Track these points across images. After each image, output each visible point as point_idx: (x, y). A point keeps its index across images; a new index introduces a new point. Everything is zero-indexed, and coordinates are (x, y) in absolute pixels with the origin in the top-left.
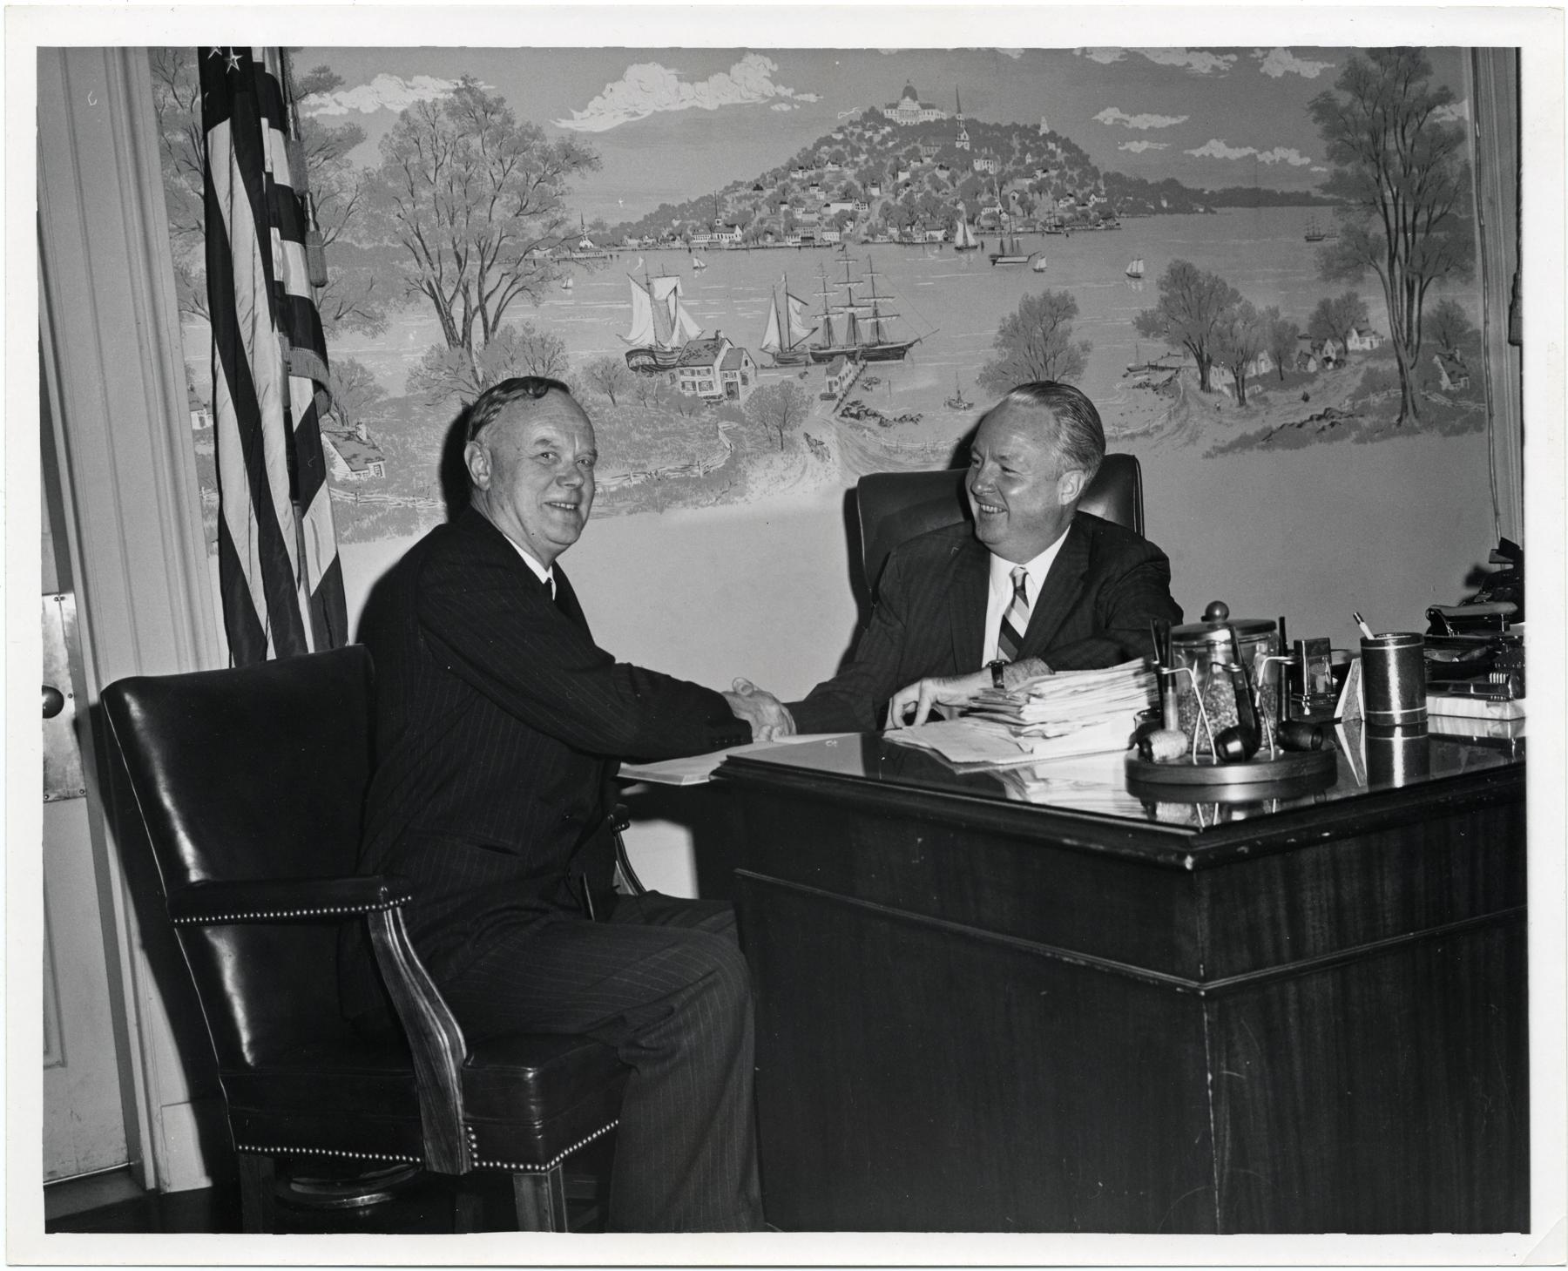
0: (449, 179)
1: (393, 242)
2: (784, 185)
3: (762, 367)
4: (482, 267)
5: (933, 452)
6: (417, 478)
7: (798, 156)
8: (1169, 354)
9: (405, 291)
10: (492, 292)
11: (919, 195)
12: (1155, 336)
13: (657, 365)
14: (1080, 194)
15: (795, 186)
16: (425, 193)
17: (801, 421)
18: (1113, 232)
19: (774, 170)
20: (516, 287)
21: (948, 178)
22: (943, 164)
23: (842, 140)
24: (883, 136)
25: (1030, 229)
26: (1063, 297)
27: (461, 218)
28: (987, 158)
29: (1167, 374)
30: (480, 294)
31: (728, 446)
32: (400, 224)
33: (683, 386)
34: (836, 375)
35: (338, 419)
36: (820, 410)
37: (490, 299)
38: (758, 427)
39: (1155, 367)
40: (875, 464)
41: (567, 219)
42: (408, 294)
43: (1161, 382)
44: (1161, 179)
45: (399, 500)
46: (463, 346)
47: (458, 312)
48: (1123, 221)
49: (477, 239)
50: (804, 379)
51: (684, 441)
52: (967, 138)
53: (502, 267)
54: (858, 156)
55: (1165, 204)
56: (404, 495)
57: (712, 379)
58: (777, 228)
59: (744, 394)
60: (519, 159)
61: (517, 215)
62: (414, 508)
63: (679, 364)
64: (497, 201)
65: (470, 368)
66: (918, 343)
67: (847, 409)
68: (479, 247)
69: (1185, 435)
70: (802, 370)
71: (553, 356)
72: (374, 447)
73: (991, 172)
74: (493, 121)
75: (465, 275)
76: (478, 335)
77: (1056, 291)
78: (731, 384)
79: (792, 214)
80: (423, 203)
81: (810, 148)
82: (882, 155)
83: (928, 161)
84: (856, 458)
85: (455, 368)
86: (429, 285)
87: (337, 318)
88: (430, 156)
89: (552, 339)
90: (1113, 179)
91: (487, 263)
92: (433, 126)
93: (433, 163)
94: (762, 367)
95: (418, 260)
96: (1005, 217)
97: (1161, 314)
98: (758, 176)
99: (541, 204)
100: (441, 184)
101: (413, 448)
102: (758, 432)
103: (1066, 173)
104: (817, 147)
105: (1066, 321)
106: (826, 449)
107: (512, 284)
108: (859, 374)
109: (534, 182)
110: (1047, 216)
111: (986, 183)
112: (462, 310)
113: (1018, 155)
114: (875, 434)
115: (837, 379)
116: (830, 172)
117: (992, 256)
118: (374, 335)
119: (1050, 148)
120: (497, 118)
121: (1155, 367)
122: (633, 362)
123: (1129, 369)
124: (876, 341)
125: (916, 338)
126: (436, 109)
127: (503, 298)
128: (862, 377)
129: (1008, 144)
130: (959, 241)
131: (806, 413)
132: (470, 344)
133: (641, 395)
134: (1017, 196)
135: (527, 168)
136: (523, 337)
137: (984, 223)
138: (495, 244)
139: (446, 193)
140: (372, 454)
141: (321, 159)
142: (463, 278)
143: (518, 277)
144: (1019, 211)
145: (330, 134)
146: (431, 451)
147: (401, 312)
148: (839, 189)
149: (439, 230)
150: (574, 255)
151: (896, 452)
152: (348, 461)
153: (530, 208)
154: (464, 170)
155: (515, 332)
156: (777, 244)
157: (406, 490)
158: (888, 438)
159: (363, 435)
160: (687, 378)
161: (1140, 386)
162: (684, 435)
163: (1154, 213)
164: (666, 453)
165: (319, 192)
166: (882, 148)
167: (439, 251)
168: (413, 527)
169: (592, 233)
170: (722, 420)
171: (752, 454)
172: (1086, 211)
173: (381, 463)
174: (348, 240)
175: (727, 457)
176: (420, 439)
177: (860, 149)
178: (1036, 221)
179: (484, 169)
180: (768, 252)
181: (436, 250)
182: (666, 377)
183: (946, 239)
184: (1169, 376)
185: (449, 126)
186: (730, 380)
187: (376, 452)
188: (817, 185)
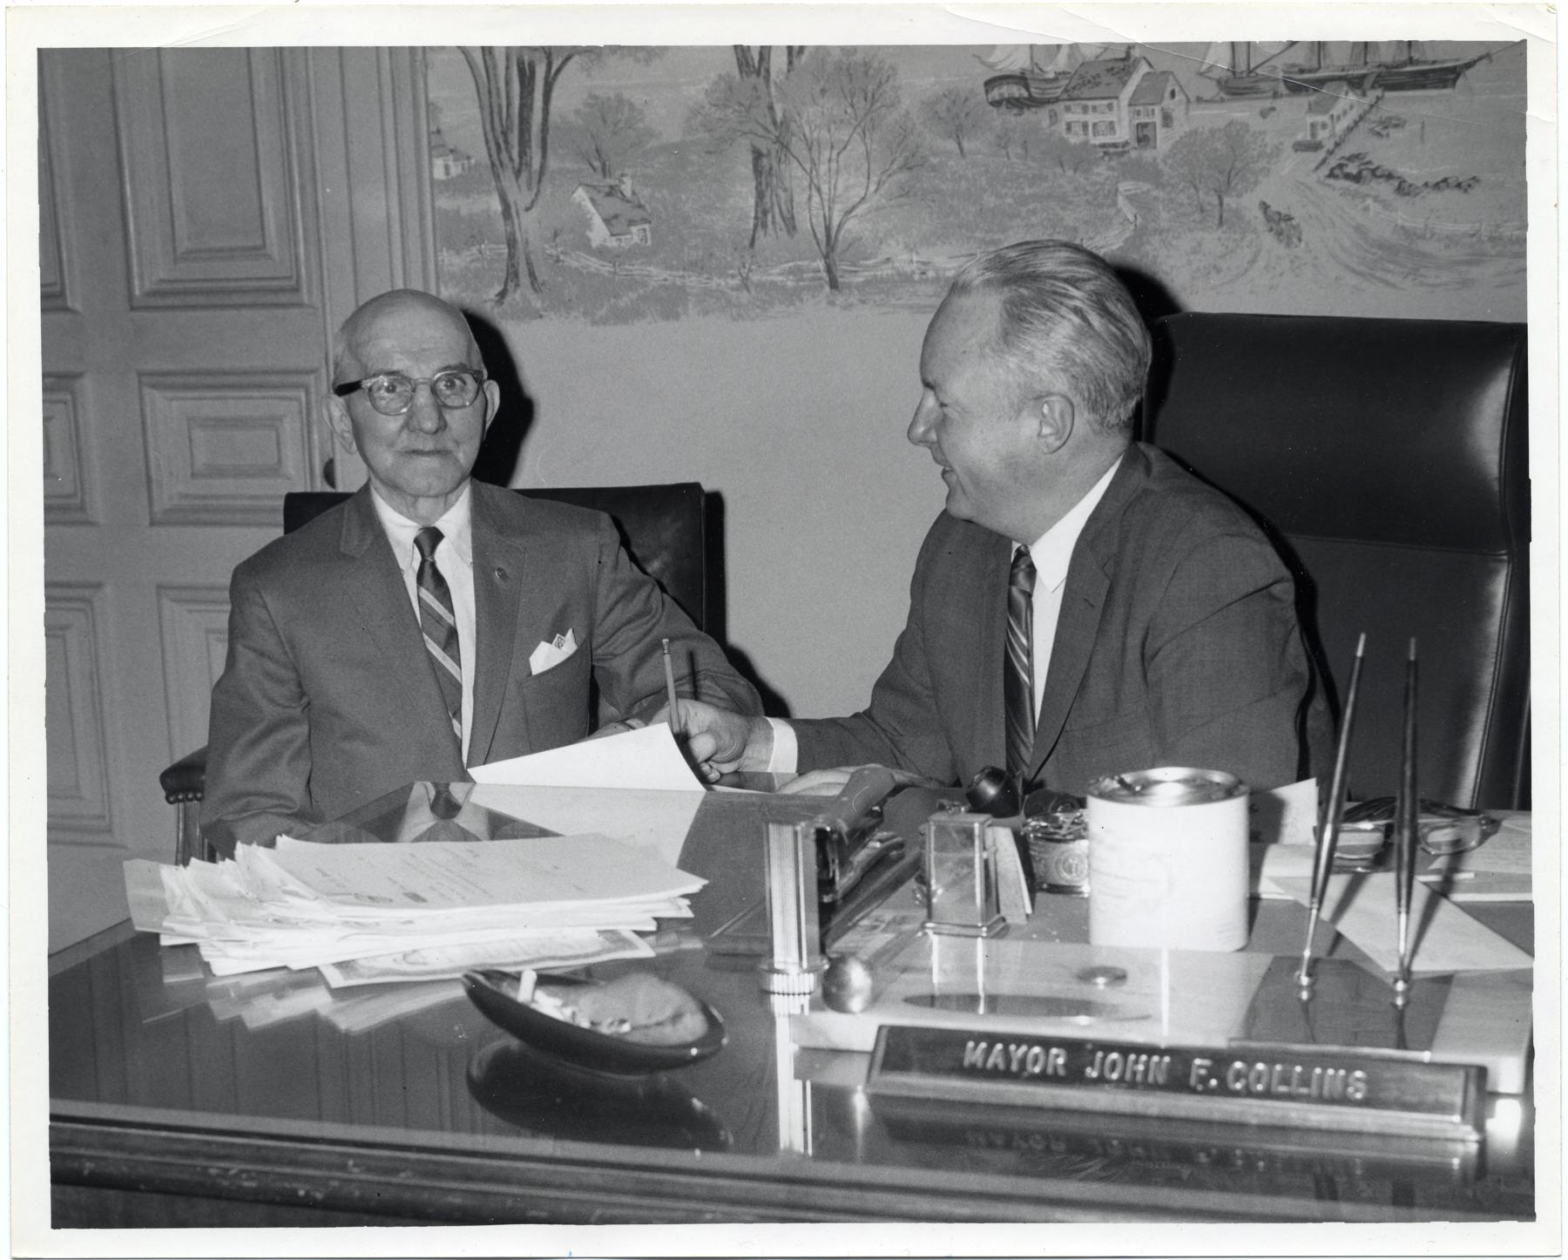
3: (1199, 100)
5: (1491, 239)
13: (1031, 98)
17: (1256, 183)
31: (1131, 218)
33: (1069, 128)
34: (1326, 112)
35: (599, 170)
36: (1291, 165)
38: (1182, 190)
40: (1380, 252)
45: (666, 274)
46: (758, 74)
50: (1268, 120)
51: (1063, 209)
56: (670, 268)
57: (1115, 119)
59: (1164, 140)
62: (682, 288)
63: (1065, 96)
66: (1485, 61)
67: (1340, 166)
70: (1268, 104)
72: (640, 206)
78: (1144, 126)
84: (1347, 244)
85: (747, 103)
89: (880, 63)
94: (1199, 100)
102: (1182, 198)
106: (1295, 228)
108: (1366, 113)
114: (1386, 205)
115: (1325, 118)
122: (995, 94)
124: (1404, 57)
125: (1484, 53)
128: (1373, 116)
131: (1266, 171)
132: (768, 71)
133: (1003, 141)
140: (637, 214)
146: (708, 213)
151: (1423, 237)
152: (607, 221)
158: (1405, 214)
159: (627, 188)
160: (1075, 116)
162: (1064, 201)
164: (1033, 226)
168: (680, 310)
170: (1125, 178)
171: (1168, 230)
173: (646, 226)
175: (1128, 234)
182: (1041, 116)
186: (1143, 120)
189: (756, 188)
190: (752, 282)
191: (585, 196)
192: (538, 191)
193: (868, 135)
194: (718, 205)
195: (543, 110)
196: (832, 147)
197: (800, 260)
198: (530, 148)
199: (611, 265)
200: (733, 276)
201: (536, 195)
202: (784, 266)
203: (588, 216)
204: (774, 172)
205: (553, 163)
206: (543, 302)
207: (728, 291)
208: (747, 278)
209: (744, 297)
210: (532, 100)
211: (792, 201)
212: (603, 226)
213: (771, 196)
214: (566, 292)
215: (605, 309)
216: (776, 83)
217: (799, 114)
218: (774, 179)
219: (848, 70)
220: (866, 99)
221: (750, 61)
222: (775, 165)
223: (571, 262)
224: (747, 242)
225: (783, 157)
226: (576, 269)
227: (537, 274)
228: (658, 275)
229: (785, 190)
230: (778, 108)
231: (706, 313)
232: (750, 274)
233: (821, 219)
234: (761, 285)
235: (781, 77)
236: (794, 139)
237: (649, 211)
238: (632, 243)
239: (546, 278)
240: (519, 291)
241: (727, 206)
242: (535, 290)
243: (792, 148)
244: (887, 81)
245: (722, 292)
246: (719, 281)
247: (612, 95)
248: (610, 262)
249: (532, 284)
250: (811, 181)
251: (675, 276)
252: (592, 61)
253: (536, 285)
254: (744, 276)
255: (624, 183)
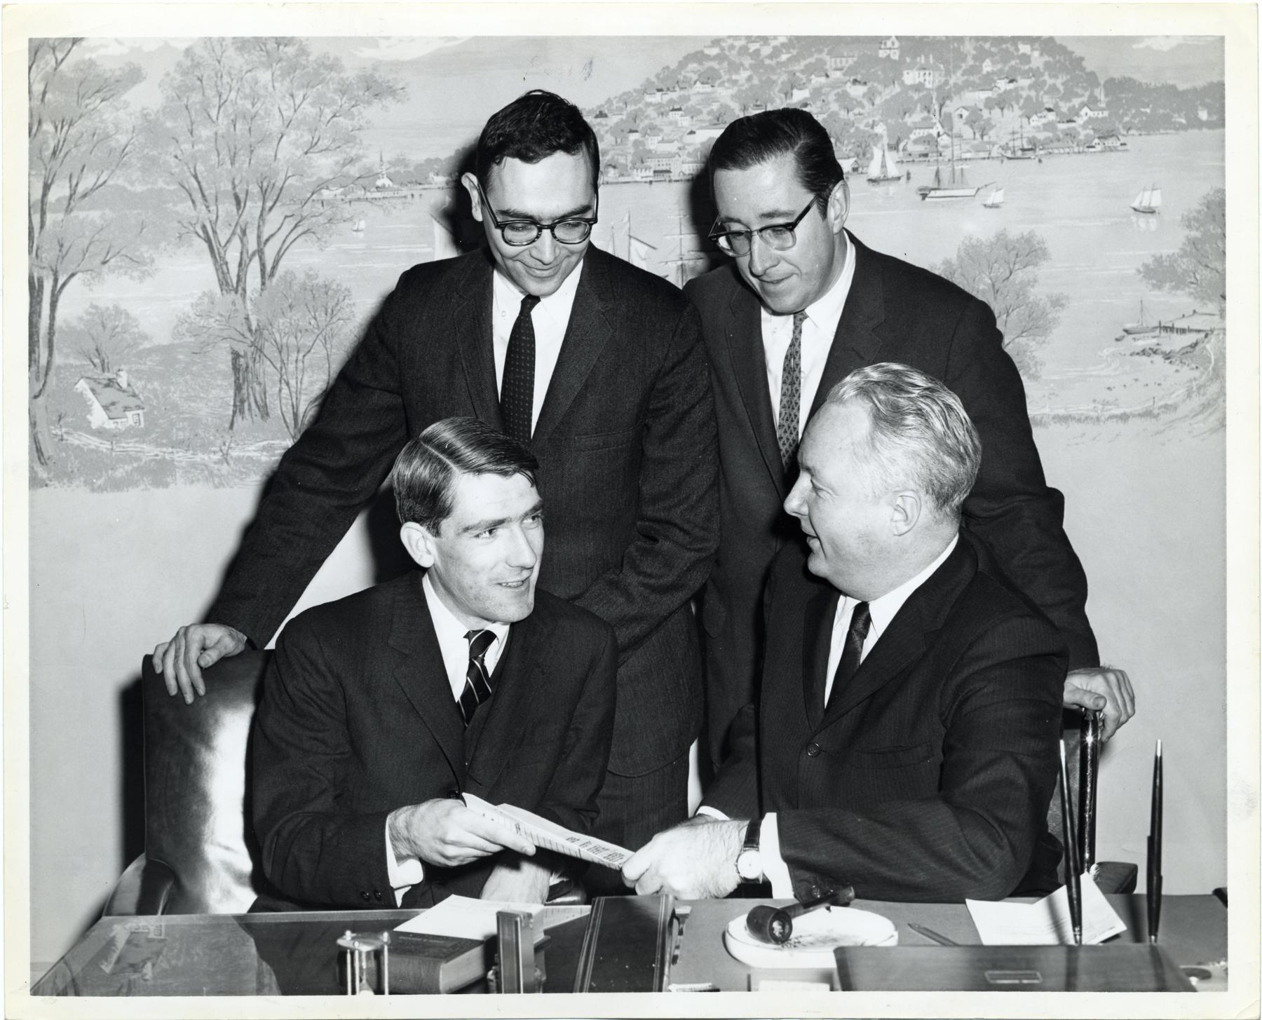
0: (233, 117)
1: (168, 184)
2: (634, 110)
4: (263, 209)
6: (178, 429)
7: (657, 76)
8: (1195, 312)
9: (177, 235)
10: (272, 236)
11: (825, 116)
12: (1177, 287)
14: (1064, 107)
15: (651, 112)
16: (205, 132)
18: (1113, 154)
19: (624, 94)
20: (300, 230)
21: (864, 95)
22: (859, 78)
23: (718, 54)
24: (775, 48)
25: (982, 155)
26: (1028, 240)
27: (242, 158)
28: (924, 69)
29: (1190, 338)
30: (259, 237)
32: (177, 166)
35: (99, 365)
37: (270, 243)
39: (1171, 329)
41: (362, 157)
42: (180, 237)
43: (1178, 349)
44: (1200, 83)
45: (157, 451)
46: (236, 292)
47: (233, 256)
48: (1134, 140)
49: (260, 180)
52: (897, 44)
53: (286, 207)
54: (737, 72)
55: (1203, 115)
56: (162, 445)
58: (622, 160)
60: (312, 93)
61: (306, 153)
62: (173, 460)
64: (284, 139)
65: (244, 316)
68: (261, 188)
69: (1212, 418)
71: (337, 304)
72: (134, 395)
73: (928, 86)
74: (286, 53)
75: (243, 218)
76: (253, 279)
77: (1016, 232)
79: (643, 144)
80: (203, 143)
81: (673, 66)
82: (772, 69)
83: (838, 74)
85: (227, 315)
86: (204, 227)
87: (104, 263)
88: (214, 93)
89: (338, 285)
90: (1118, 87)
91: (269, 204)
92: (219, 62)
93: (216, 101)
95: (193, 202)
96: (944, 140)
97: (1185, 260)
98: (603, 103)
99: (334, 140)
100: (223, 123)
101: (175, 397)
103: (1045, 82)
104: (682, 65)
105: (1030, 268)
107: (296, 226)
109: (328, 118)
110: (1010, 137)
111: (920, 100)
112: (238, 255)
113: (970, 62)
116: (698, 93)
117: (920, 190)
118: (141, 279)
119: (1021, 52)
120: (291, 50)
121: (1171, 329)
123: (1126, 331)
126: (224, 43)
127: (284, 241)
129: (959, 48)
130: (874, 170)
132: (244, 290)
134: (965, 114)
135: (320, 102)
136: (304, 283)
137: (912, 148)
138: (279, 184)
139: (228, 131)
140: (132, 402)
141: (99, 101)
142: (242, 223)
143: (303, 219)
144: (967, 132)
145: (108, 75)
146: (194, 401)
147: (171, 257)
148: (709, 113)
149: (218, 171)
150: (369, 195)
152: (106, 408)
153: (324, 143)
154: (250, 106)
155: (295, 278)
156: (622, 179)
157: (164, 441)
159: (123, 380)
161: (1144, 352)
163: (1184, 127)
165: (94, 135)
166: (773, 62)
167: (217, 193)
168: (169, 479)
169: (392, 170)
172: (1074, 129)
173: (140, 412)
174: (121, 182)
176: (184, 389)
177: (742, 65)
178: (993, 144)
179: (273, 105)
180: (609, 186)
181: (213, 191)
183: (855, 170)
184: (1195, 341)
185: (237, 61)
187: (134, 399)
188: (680, 109)
189: (235, 382)
190: (231, 457)
191: (87, 387)
192: (45, 382)
193: (328, 342)
194: (202, 395)
195: (50, 316)
196: (298, 352)
197: (272, 440)
198: (38, 347)
200: (215, 452)
201: (44, 385)
202: (258, 444)
203: (89, 403)
204: (250, 369)
205: (58, 360)
206: (48, 474)
207: (212, 465)
208: (227, 454)
209: (225, 469)
210: (40, 308)
211: (265, 393)
212: (101, 409)
213: (248, 389)
214: (69, 465)
215: (103, 479)
216: (251, 300)
217: (271, 324)
218: (250, 375)
219: (312, 291)
220: (326, 314)
221: (229, 281)
222: (251, 364)
223: (75, 440)
224: (227, 426)
225: (258, 358)
226: (78, 446)
227: (43, 450)
228: (149, 451)
229: (260, 384)
230: (253, 320)
231: (192, 482)
233: (290, 408)
234: (239, 459)
235: (256, 295)
236: (267, 344)
237: (142, 399)
238: (128, 425)
239: (51, 453)
241: (211, 396)
242: (42, 464)
243: (265, 352)
244: (344, 299)
245: (206, 466)
246: (202, 456)
247: (111, 307)
248: (108, 441)
249: (39, 459)
250: (281, 377)
251: (165, 452)
252: (93, 278)
253: (43, 461)
254: (225, 452)
255: (120, 376)
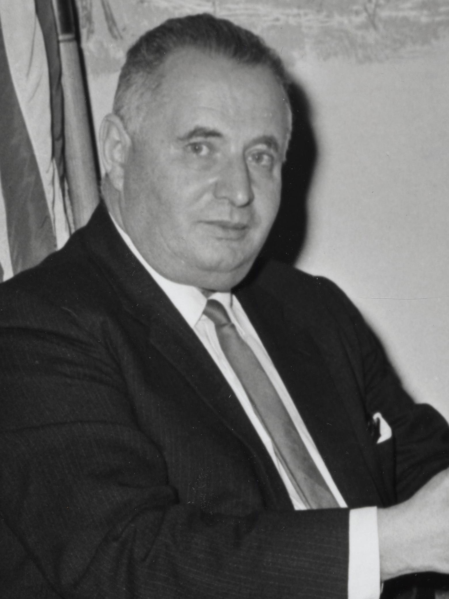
45: (277, 13)
62: (300, 26)
199: (210, 4)
200: (357, 13)
208: (374, 15)
209: (371, 36)
227: (116, 17)
232: (378, 10)
240: (94, 38)
242: (115, 37)
249: (110, 30)
251: (288, 15)
253: (116, 33)
254: (371, 11)
